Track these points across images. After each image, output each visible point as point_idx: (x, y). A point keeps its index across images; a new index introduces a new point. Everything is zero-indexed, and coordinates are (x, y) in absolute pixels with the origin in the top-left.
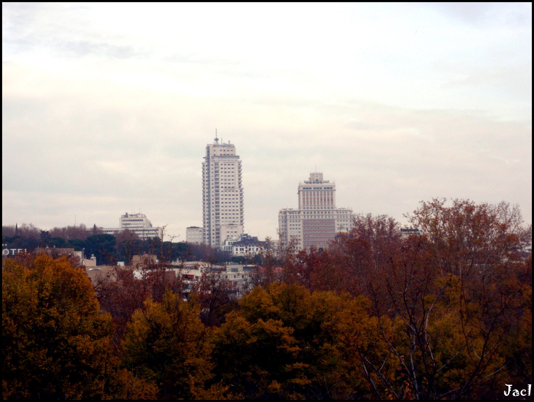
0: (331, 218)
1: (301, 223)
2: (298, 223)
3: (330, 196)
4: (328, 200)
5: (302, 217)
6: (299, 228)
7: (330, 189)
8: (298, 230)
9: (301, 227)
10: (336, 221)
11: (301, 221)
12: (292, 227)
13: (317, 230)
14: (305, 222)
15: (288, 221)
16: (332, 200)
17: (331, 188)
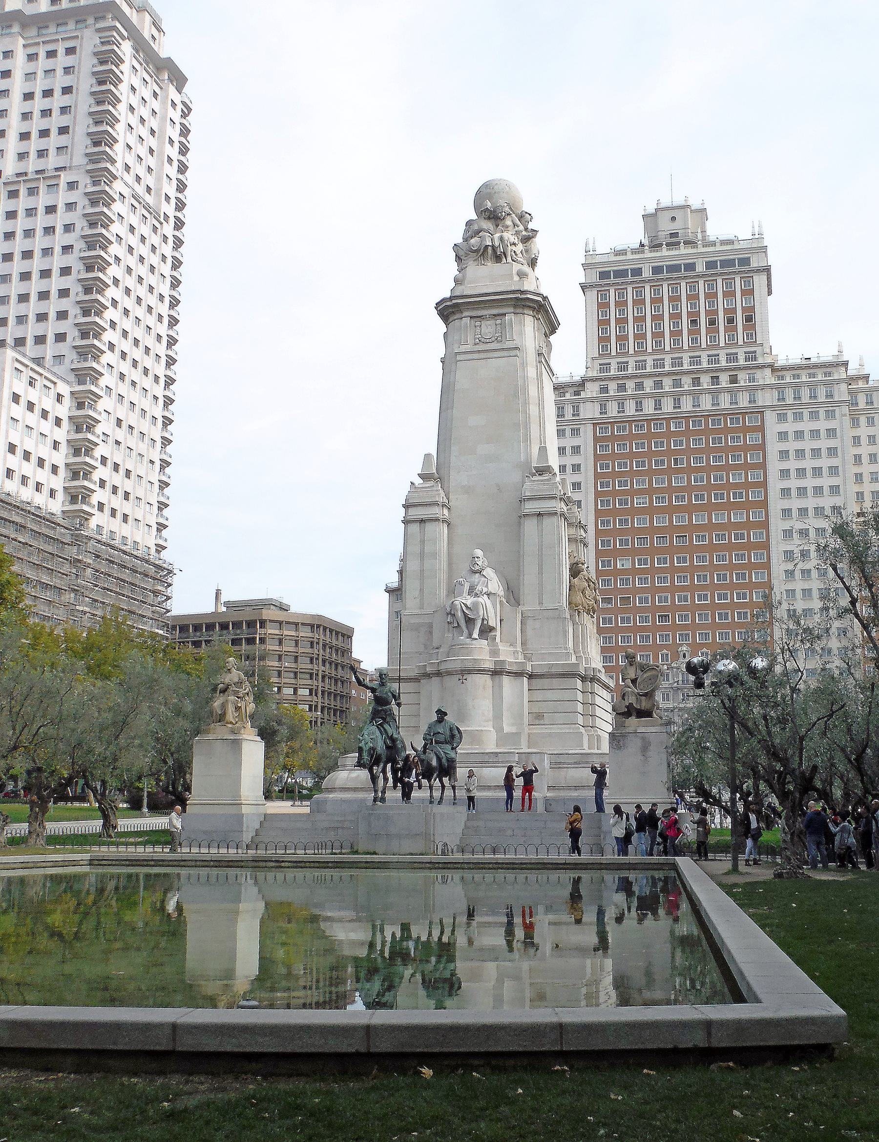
0: (743, 401)
7: (742, 269)
10: (770, 417)
11: (587, 432)
13: (670, 471)
16: (749, 319)
17: (745, 262)
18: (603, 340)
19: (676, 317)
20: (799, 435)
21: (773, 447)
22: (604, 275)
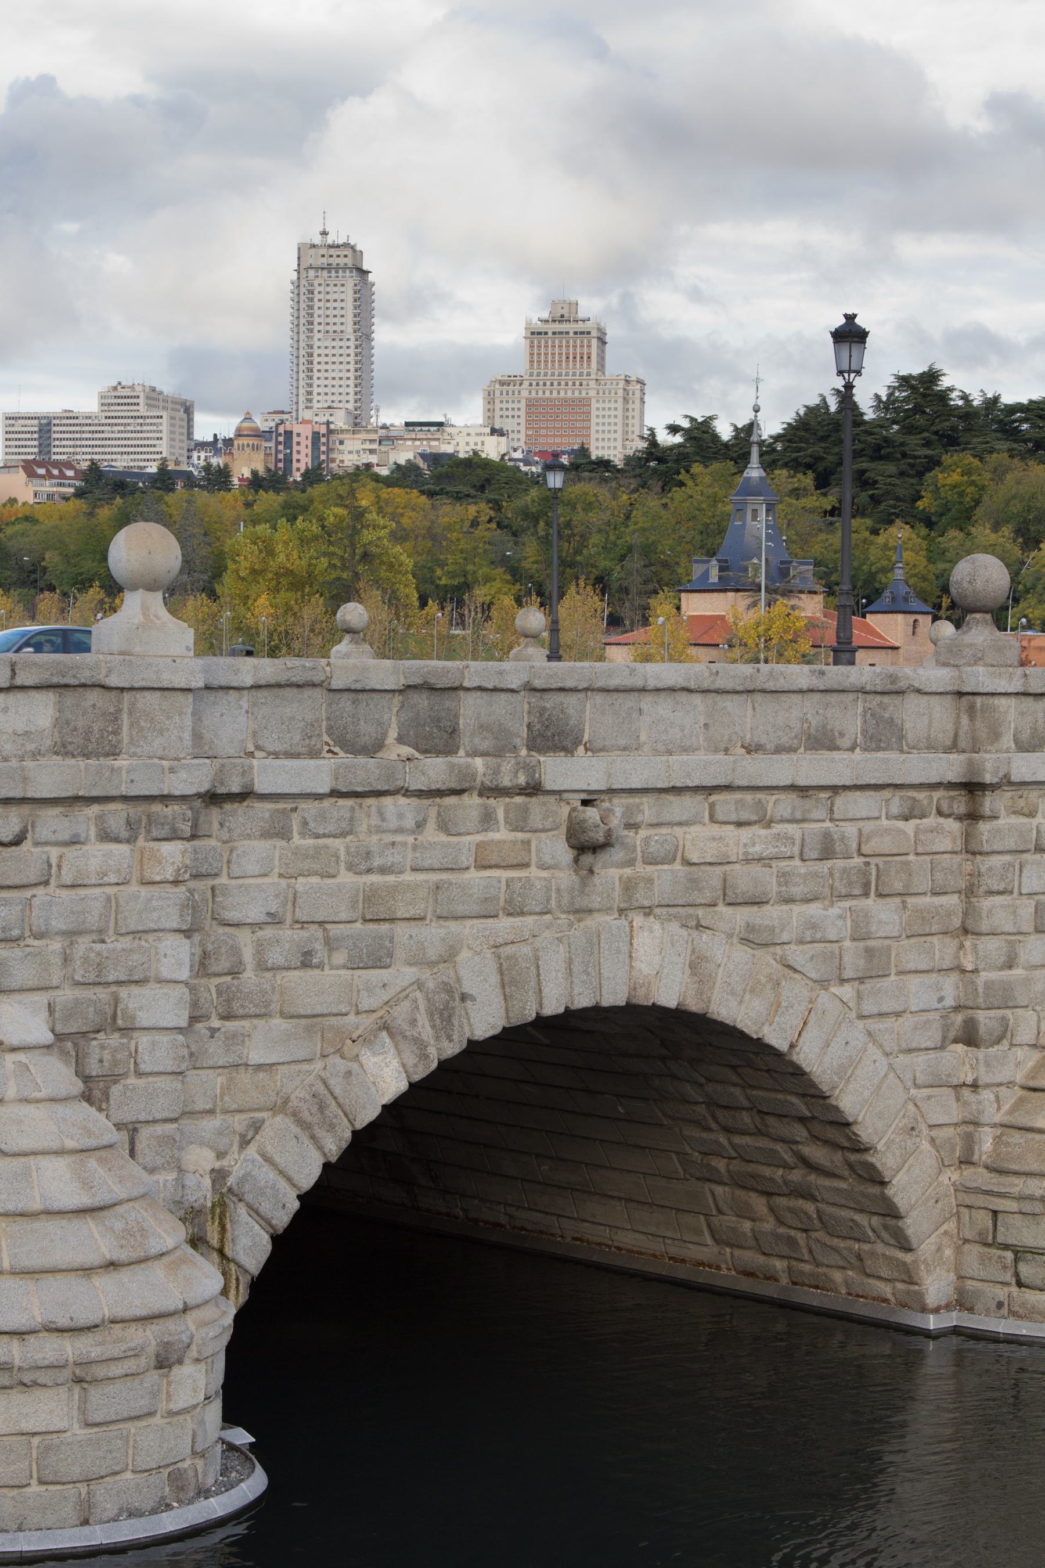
0: (584, 395)
1: (523, 405)
2: (516, 406)
3: (585, 350)
4: (582, 358)
5: (525, 394)
6: (519, 417)
8: (516, 420)
9: (522, 413)
10: (593, 401)
11: (523, 402)
12: (505, 413)
13: (554, 421)
14: (531, 404)
15: (497, 401)
16: (589, 358)
17: (589, 333)
18: (532, 362)
19: (560, 354)
20: (604, 409)
21: (594, 413)
22: (533, 333)
